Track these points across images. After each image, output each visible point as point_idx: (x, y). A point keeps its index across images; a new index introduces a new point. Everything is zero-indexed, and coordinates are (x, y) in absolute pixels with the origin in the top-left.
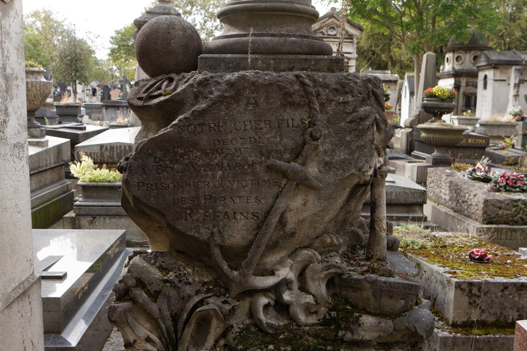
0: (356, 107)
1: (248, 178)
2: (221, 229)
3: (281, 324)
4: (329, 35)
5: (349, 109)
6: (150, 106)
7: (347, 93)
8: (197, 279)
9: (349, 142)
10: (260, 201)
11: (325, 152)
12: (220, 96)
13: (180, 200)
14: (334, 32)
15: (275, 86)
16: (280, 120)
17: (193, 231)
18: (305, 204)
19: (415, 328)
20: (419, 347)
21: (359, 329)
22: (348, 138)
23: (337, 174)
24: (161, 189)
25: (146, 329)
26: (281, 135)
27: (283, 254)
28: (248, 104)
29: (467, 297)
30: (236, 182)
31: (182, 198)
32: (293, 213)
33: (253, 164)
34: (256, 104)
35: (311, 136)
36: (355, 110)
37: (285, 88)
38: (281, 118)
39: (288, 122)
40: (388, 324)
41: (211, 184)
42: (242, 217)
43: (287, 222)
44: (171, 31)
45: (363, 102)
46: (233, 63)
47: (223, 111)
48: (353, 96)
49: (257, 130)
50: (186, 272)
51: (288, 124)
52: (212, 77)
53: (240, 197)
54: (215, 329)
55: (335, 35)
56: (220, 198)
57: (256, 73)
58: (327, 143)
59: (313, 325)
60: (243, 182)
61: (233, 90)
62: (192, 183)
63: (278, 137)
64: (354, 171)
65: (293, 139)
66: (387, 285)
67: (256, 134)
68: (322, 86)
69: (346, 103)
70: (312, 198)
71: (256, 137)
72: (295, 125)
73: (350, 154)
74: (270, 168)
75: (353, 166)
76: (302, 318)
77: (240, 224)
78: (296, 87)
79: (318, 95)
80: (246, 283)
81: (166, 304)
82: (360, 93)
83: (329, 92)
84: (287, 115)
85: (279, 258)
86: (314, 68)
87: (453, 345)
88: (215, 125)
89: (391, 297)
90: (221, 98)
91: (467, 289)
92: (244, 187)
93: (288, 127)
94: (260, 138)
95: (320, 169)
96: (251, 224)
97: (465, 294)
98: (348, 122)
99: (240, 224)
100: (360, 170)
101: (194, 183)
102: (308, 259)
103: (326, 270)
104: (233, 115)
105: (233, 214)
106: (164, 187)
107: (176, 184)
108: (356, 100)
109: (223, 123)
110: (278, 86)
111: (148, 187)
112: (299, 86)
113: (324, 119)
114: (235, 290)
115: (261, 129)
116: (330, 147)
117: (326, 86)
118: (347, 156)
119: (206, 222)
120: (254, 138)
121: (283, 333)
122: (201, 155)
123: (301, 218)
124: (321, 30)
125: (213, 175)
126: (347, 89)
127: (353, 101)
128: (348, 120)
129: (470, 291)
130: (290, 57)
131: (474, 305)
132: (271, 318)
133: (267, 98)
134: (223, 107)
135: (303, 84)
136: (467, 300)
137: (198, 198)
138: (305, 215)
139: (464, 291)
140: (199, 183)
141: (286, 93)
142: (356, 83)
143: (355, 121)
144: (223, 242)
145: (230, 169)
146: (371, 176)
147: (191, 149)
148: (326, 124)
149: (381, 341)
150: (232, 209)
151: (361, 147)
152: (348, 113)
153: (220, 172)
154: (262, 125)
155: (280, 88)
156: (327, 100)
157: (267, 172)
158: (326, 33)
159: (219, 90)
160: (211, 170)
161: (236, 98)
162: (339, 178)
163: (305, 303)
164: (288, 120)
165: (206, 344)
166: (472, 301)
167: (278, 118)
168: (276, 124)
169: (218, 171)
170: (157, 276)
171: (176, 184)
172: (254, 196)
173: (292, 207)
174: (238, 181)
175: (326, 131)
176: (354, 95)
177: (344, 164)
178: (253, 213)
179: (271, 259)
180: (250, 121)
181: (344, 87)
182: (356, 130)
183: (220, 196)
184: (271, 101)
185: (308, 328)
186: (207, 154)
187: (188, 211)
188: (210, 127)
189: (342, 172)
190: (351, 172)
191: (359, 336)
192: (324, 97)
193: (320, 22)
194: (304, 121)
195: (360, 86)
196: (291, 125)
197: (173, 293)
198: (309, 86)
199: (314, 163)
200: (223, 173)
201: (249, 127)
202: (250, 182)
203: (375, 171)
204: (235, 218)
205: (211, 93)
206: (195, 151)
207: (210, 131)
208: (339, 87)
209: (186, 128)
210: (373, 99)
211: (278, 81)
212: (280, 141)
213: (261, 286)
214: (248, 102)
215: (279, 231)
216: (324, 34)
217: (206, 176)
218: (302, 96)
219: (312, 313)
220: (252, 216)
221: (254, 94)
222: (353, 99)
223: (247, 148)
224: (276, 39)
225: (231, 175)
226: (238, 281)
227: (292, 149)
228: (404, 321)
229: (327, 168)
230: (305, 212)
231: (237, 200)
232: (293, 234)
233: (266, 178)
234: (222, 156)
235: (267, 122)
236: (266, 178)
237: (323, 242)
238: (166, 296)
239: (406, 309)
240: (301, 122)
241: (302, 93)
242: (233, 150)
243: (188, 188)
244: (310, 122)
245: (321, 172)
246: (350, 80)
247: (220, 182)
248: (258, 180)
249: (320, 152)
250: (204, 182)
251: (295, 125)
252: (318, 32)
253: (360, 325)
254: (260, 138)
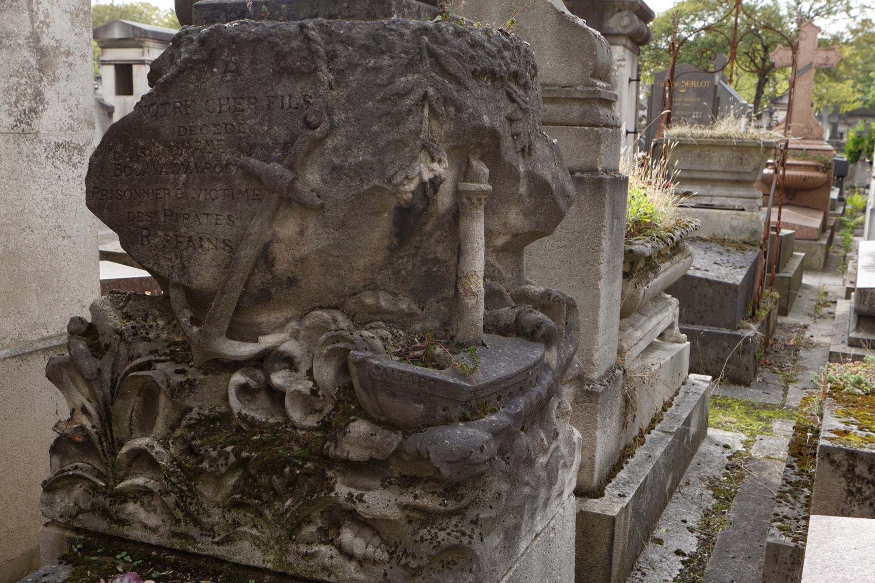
1: (219, 186)
2: (186, 263)
3: (272, 421)
5: (383, 78)
7: (383, 53)
8: (164, 336)
9: (376, 133)
10: (233, 222)
11: (335, 150)
13: (136, 214)
15: (266, 43)
16: (272, 97)
17: (152, 262)
18: (301, 233)
19: (428, 453)
20: (459, 492)
21: (344, 440)
22: (375, 128)
23: (350, 187)
24: (117, 198)
25: (83, 395)
26: (270, 121)
27: (289, 313)
28: (225, 72)
29: (843, 479)
30: (203, 192)
31: (138, 213)
32: (283, 245)
33: (227, 165)
34: (237, 72)
36: (391, 81)
37: (277, 44)
38: (272, 94)
39: (282, 100)
40: (395, 439)
41: (173, 194)
42: (211, 246)
43: (274, 259)
45: (411, 66)
46: (235, 13)
47: (192, 83)
48: (392, 58)
49: (237, 111)
50: (154, 324)
51: (283, 104)
53: (208, 215)
54: (164, 410)
56: (183, 214)
57: (242, 23)
58: (340, 135)
59: (311, 429)
60: (212, 192)
61: (205, 51)
62: (151, 191)
63: (266, 124)
64: (377, 182)
65: (287, 128)
66: (380, 371)
67: (235, 118)
68: (342, 42)
69: (377, 69)
70: (312, 223)
71: (234, 124)
73: (374, 155)
74: (250, 174)
75: (376, 174)
76: (296, 415)
77: (208, 256)
79: (332, 57)
80: (208, 346)
81: (110, 364)
82: (406, 53)
83: (354, 51)
84: (282, 89)
85: (282, 320)
86: (346, 14)
87: (792, 564)
88: (182, 105)
89: (394, 395)
90: (190, 63)
91: (846, 463)
92: (213, 199)
93: (282, 107)
94: (240, 124)
95: (324, 177)
96: (222, 257)
97: (839, 473)
98: (378, 101)
99: (208, 256)
100: (390, 181)
101: (153, 190)
102: (322, 324)
103: (333, 343)
104: (205, 89)
105: (198, 240)
106: (120, 195)
107: (133, 191)
108: (395, 63)
109: (192, 101)
110: (269, 42)
111: (103, 195)
112: (302, 41)
113: (342, 96)
114: (197, 357)
115: (243, 111)
116: (345, 141)
117: (347, 41)
118: (368, 158)
119: (167, 250)
120: (232, 125)
121: (261, 433)
122: (164, 150)
123: (298, 255)
125: (175, 179)
127: (390, 66)
128: (379, 98)
129: (852, 469)
131: (858, 496)
132: (258, 409)
133: (254, 62)
134: (193, 76)
135: (308, 39)
136: (844, 484)
137: (156, 213)
138: (304, 250)
139: (838, 466)
140: (158, 192)
141: (277, 54)
142: (402, 35)
143: (389, 99)
144: (189, 282)
145: (197, 172)
146: (413, 192)
147: (153, 140)
148: (344, 105)
149: (406, 473)
150: (198, 233)
151: (399, 145)
152: (379, 85)
153: (184, 176)
154: (245, 104)
155: (273, 45)
156: (349, 63)
157: (245, 179)
160: (173, 172)
161: (210, 61)
162: (353, 192)
163: (295, 391)
164: (283, 97)
165: (154, 429)
166: (854, 489)
167: (268, 94)
168: (265, 104)
169: (182, 173)
170: (111, 324)
171: (133, 191)
172: (226, 214)
173: (280, 235)
174: (206, 190)
175: (343, 116)
176: (394, 55)
177: (361, 171)
178: (224, 240)
179: (266, 318)
180: (228, 99)
181: (378, 43)
182: (388, 114)
183: (183, 212)
184: (259, 67)
185: (303, 432)
186: (171, 148)
187: (145, 232)
188: (175, 107)
189: (358, 183)
190: (372, 184)
191: (343, 451)
192: (343, 60)
194: (308, 99)
195: (408, 41)
196: (286, 105)
197: (123, 350)
198: (314, 41)
199: (315, 166)
200: (188, 177)
201: (225, 108)
202: (221, 192)
203: (422, 184)
204: (201, 246)
206: (157, 144)
207: (175, 113)
208: (371, 43)
209: (147, 109)
210: (428, 62)
211: (270, 35)
212: (268, 130)
213: (229, 354)
214: (226, 68)
215: (265, 273)
217: (167, 181)
218: (305, 58)
219: (316, 411)
220: (222, 246)
221: (235, 55)
222: (391, 62)
223: (222, 140)
225: (197, 181)
226: (196, 342)
227: (285, 144)
228: (415, 442)
229: (335, 176)
230: (304, 245)
231: (204, 219)
232: (292, 282)
233: (243, 188)
234: (190, 152)
235: (253, 100)
236: (243, 188)
237: (362, 304)
238: (114, 352)
239: (428, 422)
240: (305, 100)
241: (305, 53)
242: (204, 142)
243: (146, 198)
245: (325, 181)
246: (391, 30)
247: (183, 190)
248: (233, 190)
249: (328, 149)
250: (164, 189)
251: (294, 105)
253: (345, 434)
254: (240, 124)
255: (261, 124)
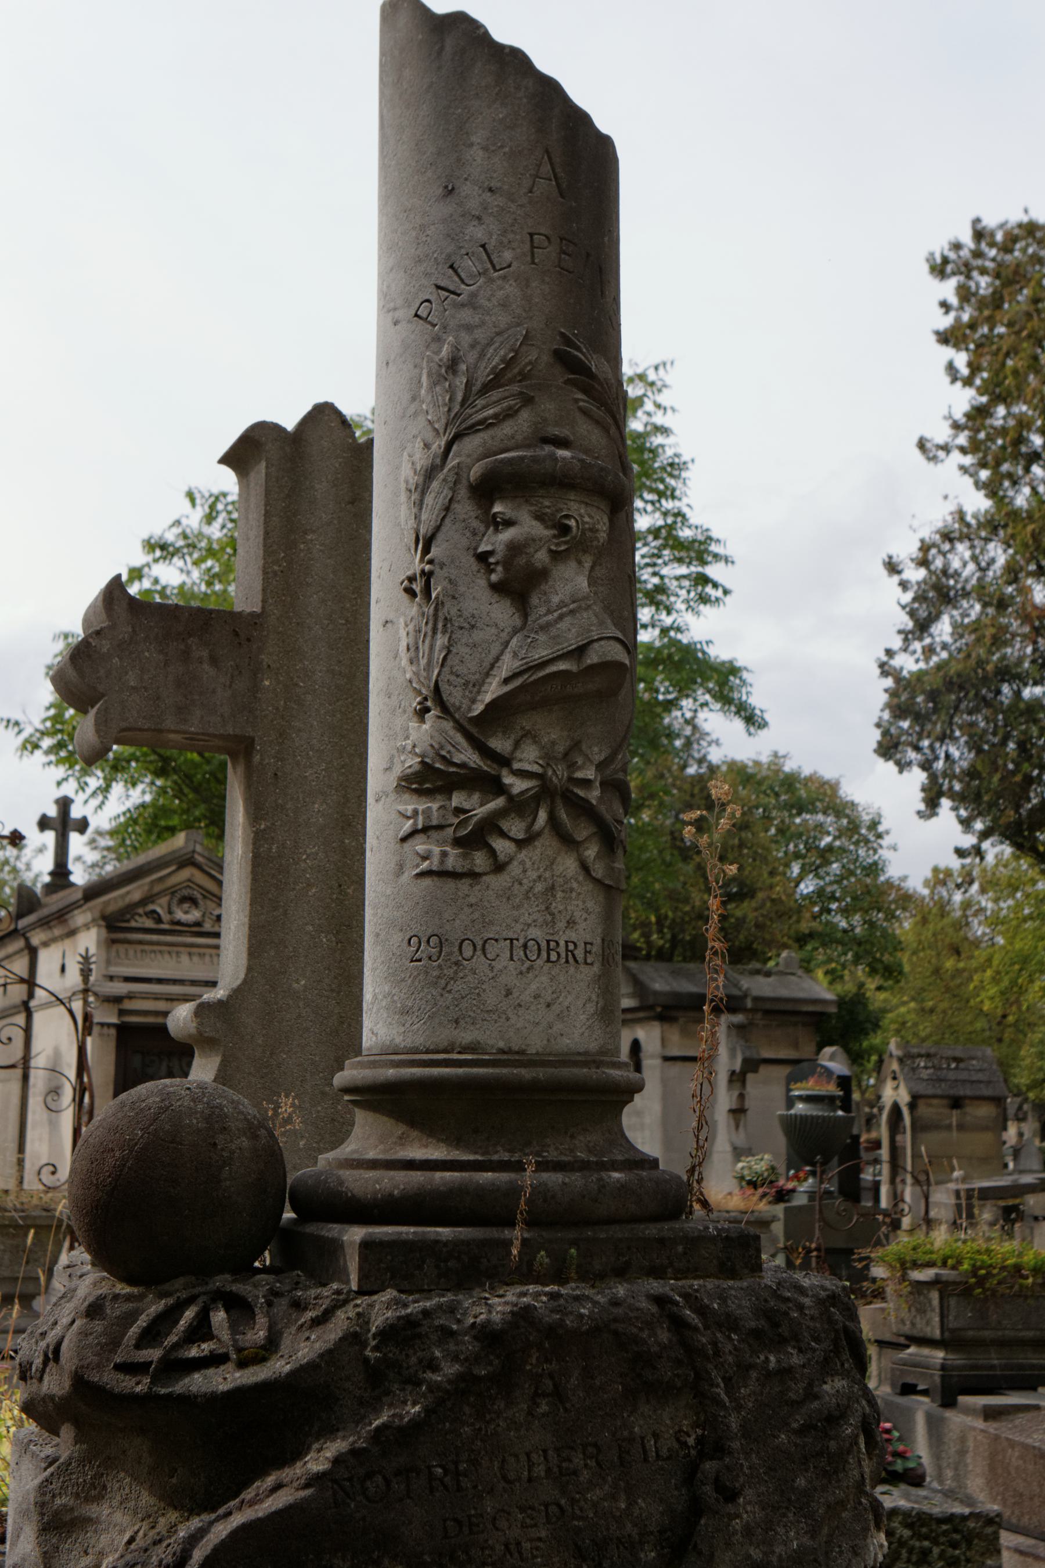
0: (810, 1385)
4: (179, 923)
5: (796, 1390)
6: (186, 1400)
11: (748, 1531)
12: (461, 1377)
14: (195, 915)
22: (801, 1482)
34: (558, 1395)
35: (719, 1486)
36: (811, 1395)
38: (626, 1433)
44: (220, 1139)
48: (800, 1350)
51: (645, 1451)
52: (426, 1313)
55: (198, 924)
63: (623, 1496)
69: (785, 1372)
71: (563, 1502)
72: (664, 1453)
78: (664, 1336)
82: (817, 1340)
84: (642, 1422)
88: (446, 1471)
93: (646, 1460)
94: (573, 1501)
108: (809, 1360)
110: (616, 1333)
112: (669, 1330)
117: (730, 1323)
124: (151, 907)
126: (784, 1330)
127: (804, 1366)
128: (795, 1425)
130: (618, 1232)
134: (467, 1410)
135: (678, 1324)
142: (801, 1307)
154: (578, 1460)
158: (165, 917)
159: (455, 1358)
164: (643, 1438)
180: (545, 1451)
181: (776, 1325)
193: (148, 880)
198: (696, 1329)
201: (540, 1470)
205: (433, 1366)
208: (762, 1323)
211: (615, 1320)
216: (159, 920)
223: (540, 1539)
224: (576, 1179)
235: (591, 1450)
240: (678, 1440)
242: (500, 1548)
244: (700, 1441)
251: (664, 1453)
252: (140, 911)
254: (573, 1501)
255: (614, 1497)
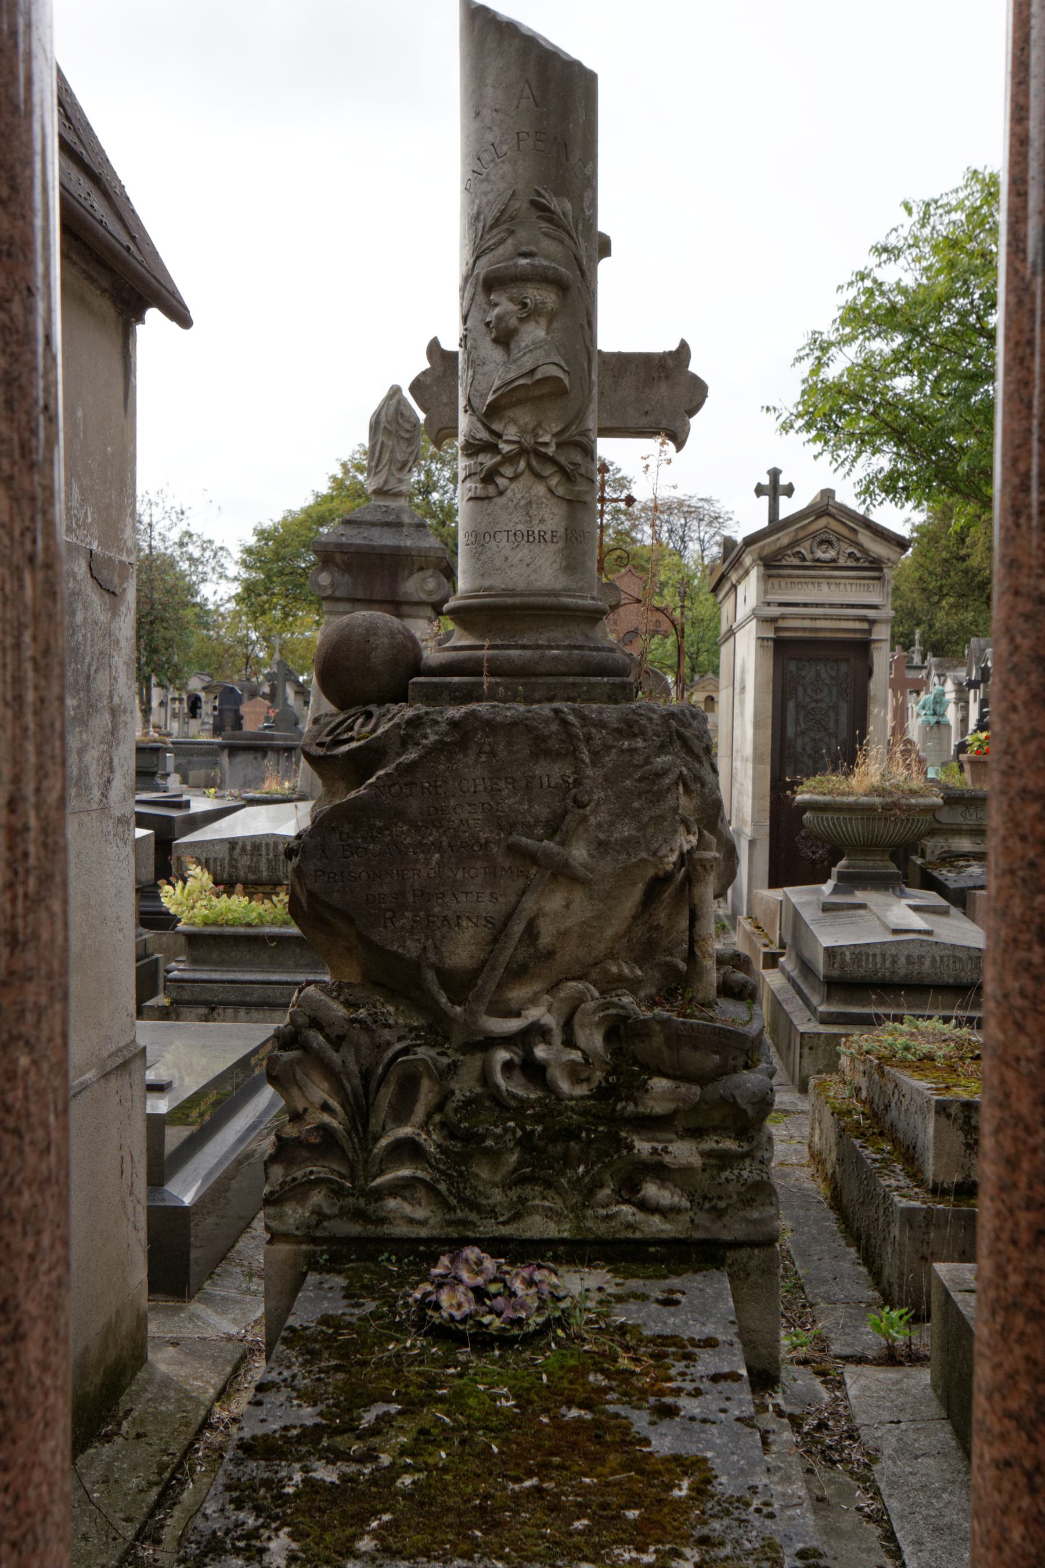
0: (649, 757)
1: (479, 864)
3: (532, 1096)
4: (818, 560)
5: (638, 759)
6: (336, 756)
7: (635, 735)
8: (401, 1021)
9: (637, 810)
11: (599, 826)
12: (437, 742)
14: (831, 554)
17: (396, 944)
18: (567, 906)
19: (734, 1097)
21: (647, 1097)
22: (636, 805)
27: (537, 986)
28: (480, 752)
29: (960, 1133)
34: (493, 753)
35: (575, 800)
36: (647, 762)
37: (536, 728)
40: (695, 1091)
41: (424, 874)
44: (372, 639)
45: (662, 749)
49: (494, 792)
52: (427, 713)
55: (834, 561)
57: (493, 707)
59: (583, 1098)
64: (644, 855)
67: (492, 798)
68: (595, 726)
69: (633, 751)
70: (578, 895)
72: (553, 784)
73: (638, 830)
74: (513, 850)
76: (565, 1086)
78: (554, 727)
79: (589, 739)
82: (658, 736)
85: (531, 994)
89: (695, 1048)
91: (961, 1115)
94: (498, 804)
100: (655, 854)
114: (458, 1037)
116: (607, 818)
117: (601, 725)
118: (634, 833)
121: (533, 1107)
123: (562, 927)
124: (797, 549)
126: (636, 730)
130: (550, 680)
135: (564, 723)
136: (962, 1138)
138: (569, 923)
142: (650, 719)
146: (674, 864)
151: (658, 820)
153: (437, 855)
154: (502, 784)
155: (530, 729)
158: (808, 556)
159: (437, 733)
168: (523, 783)
172: (488, 891)
175: (602, 794)
177: (628, 844)
179: (517, 994)
181: (630, 726)
182: (647, 792)
186: (418, 829)
187: (389, 914)
188: (423, 787)
193: (793, 528)
197: (364, 1038)
198: (573, 725)
201: (481, 788)
202: (482, 871)
203: (682, 855)
204: (458, 925)
205: (426, 737)
210: (678, 743)
216: (804, 559)
218: (564, 742)
219: (582, 1081)
222: (645, 744)
224: (528, 654)
225: (453, 860)
231: (463, 898)
232: (550, 954)
233: (507, 865)
236: (507, 865)
237: (606, 972)
239: (723, 1071)
241: (563, 736)
242: (457, 822)
243: (389, 879)
244: (575, 781)
245: (592, 856)
251: (553, 784)
252: (789, 552)
253: (647, 1091)
254: (498, 804)
255: (521, 803)
